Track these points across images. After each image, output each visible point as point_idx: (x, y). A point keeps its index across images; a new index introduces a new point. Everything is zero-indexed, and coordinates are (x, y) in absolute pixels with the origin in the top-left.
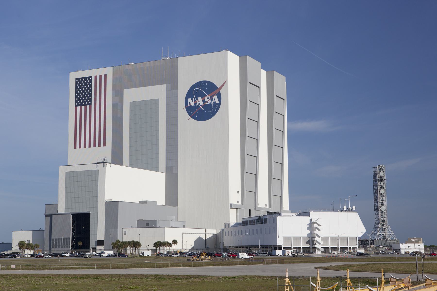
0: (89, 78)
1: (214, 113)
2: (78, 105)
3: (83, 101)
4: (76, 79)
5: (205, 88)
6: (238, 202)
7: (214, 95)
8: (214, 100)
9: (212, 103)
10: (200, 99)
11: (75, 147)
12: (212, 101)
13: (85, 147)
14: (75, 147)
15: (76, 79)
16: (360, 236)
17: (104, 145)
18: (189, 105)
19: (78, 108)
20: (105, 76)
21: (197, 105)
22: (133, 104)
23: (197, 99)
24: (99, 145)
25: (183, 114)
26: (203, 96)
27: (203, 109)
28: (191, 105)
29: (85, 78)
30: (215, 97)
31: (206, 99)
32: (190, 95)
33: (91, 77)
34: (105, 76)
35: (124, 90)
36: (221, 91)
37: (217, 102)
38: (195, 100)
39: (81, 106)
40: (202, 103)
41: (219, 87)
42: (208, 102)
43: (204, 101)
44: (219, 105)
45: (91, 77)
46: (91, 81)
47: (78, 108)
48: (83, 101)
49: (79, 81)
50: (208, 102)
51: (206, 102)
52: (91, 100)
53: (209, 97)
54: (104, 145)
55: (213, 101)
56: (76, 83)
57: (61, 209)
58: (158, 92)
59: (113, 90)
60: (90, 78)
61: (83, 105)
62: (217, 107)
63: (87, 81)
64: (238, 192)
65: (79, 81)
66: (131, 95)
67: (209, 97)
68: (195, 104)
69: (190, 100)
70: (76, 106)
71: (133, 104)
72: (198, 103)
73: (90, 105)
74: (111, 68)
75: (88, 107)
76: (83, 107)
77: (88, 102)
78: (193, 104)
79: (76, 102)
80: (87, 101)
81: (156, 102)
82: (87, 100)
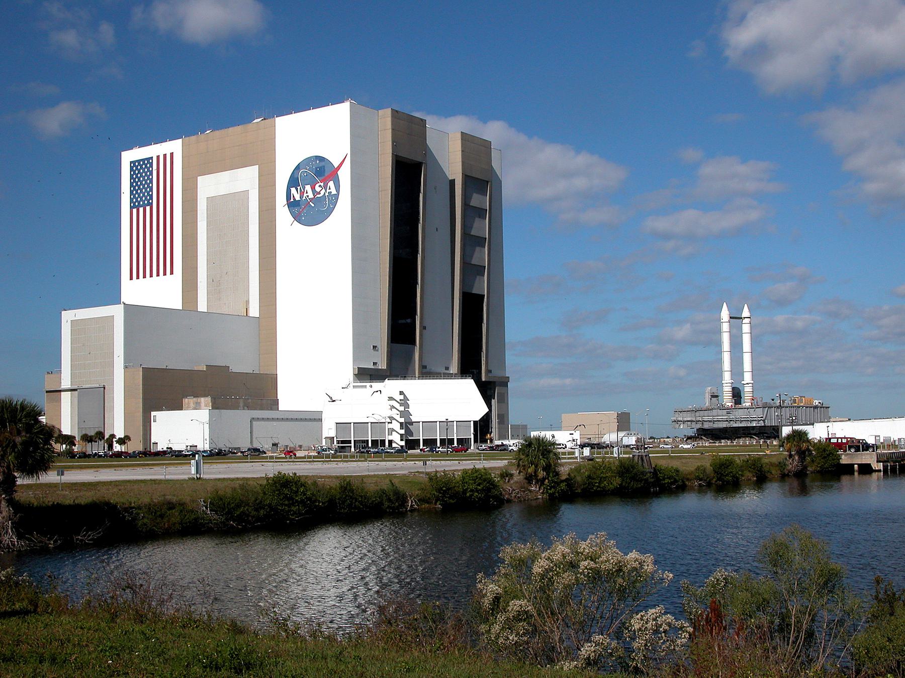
0: (148, 159)
1: (330, 211)
4: (131, 162)
5: (318, 170)
6: (375, 364)
10: (308, 188)
11: (131, 278)
14: (131, 278)
15: (131, 162)
16: (477, 419)
17: (172, 273)
20: (172, 154)
25: (283, 214)
29: (143, 160)
30: (331, 184)
31: (318, 189)
32: (294, 182)
34: (172, 154)
35: (200, 179)
37: (334, 192)
40: (311, 196)
44: (337, 196)
47: (135, 211)
49: (134, 165)
52: (151, 198)
54: (172, 273)
57: (66, 383)
58: (245, 179)
62: (334, 199)
64: (374, 347)
65: (134, 165)
66: (210, 186)
69: (293, 190)
70: (131, 208)
72: (305, 195)
74: (179, 142)
75: (148, 208)
76: (141, 209)
78: (298, 198)
81: (244, 196)
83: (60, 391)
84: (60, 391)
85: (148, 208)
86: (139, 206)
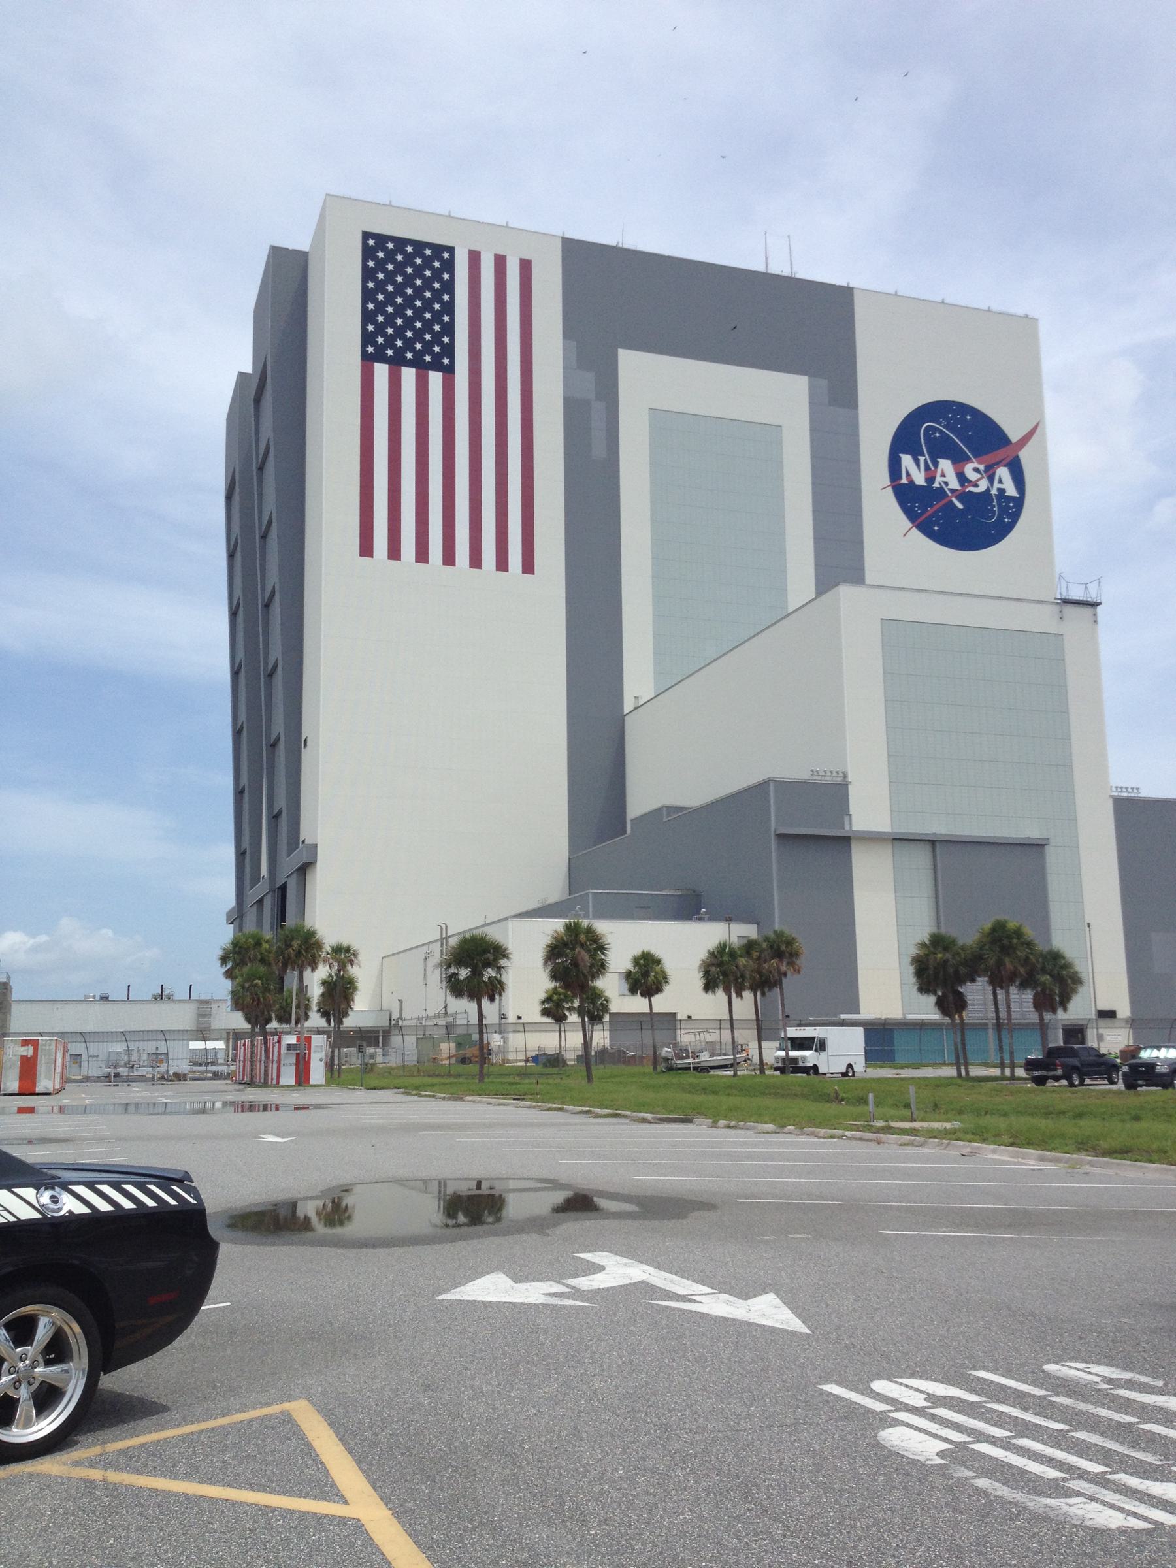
0: (438, 249)
1: (1000, 531)
2: (379, 356)
3: (409, 345)
4: (366, 235)
7: (998, 464)
8: (1000, 482)
9: (994, 492)
10: (945, 465)
11: (366, 549)
12: (991, 479)
13: (422, 555)
14: (366, 549)
15: (366, 235)
17: (528, 567)
18: (904, 481)
19: (381, 371)
20: (526, 267)
21: (936, 485)
22: (661, 419)
23: (936, 465)
24: (502, 564)
26: (959, 459)
27: (960, 506)
28: (912, 482)
29: (419, 246)
30: (1003, 472)
32: (905, 439)
33: (451, 250)
34: (526, 267)
36: (1025, 455)
37: (1011, 491)
38: (927, 468)
39: (397, 362)
40: (954, 484)
41: (1014, 436)
42: (976, 486)
43: (962, 478)
44: (1019, 502)
45: (451, 250)
46: (449, 266)
47: (381, 371)
48: (409, 345)
50: (976, 486)
51: (969, 481)
52: (449, 350)
53: (982, 467)
54: (528, 567)
55: (996, 485)
56: (368, 253)
57: (869, 811)
59: (566, 335)
60: (442, 255)
61: (409, 364)
63: (428, 262)
67: (982, 467)
68: (930, 479)
69: (907, 460)
71: (661, 419)
72: (939, 479)
73: (449, 371)
75: (435, 379)
77: (437, 358)
78: (920, 479)
79: (367, 338)
80: (428, 348)
82: (428, 348)
83: (844, 842)
84: (844, 842)
85: (435, 379)
86: (397, 362)
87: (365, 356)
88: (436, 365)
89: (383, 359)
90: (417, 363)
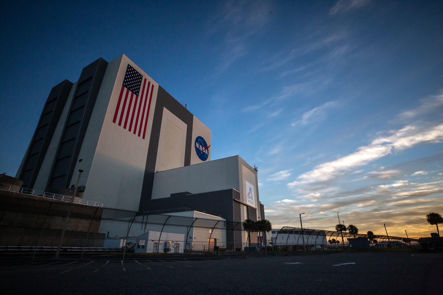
0: (140, 75)
4: (129, 65)
10: (201, 146)
11: (114, 121)
14: (114, 121)
15: (129, 65)
19: (125, 89)
20: (153, 86)
32: (197, 141)
34: (153, 86)
35: (164, 108)
39: (129, 89)
46: (141, 78)
47: (125, 89)
52: (138, 92)
56: (128, 68)
61: (131, 91)
70: (124, 86)
75: (135, 96)
76: (130, 93)
79: (124, 82)
85: (135, 96)
87: (123, 85)
88: (135, 93)
89: (127, 88)
90: (132, 91)
